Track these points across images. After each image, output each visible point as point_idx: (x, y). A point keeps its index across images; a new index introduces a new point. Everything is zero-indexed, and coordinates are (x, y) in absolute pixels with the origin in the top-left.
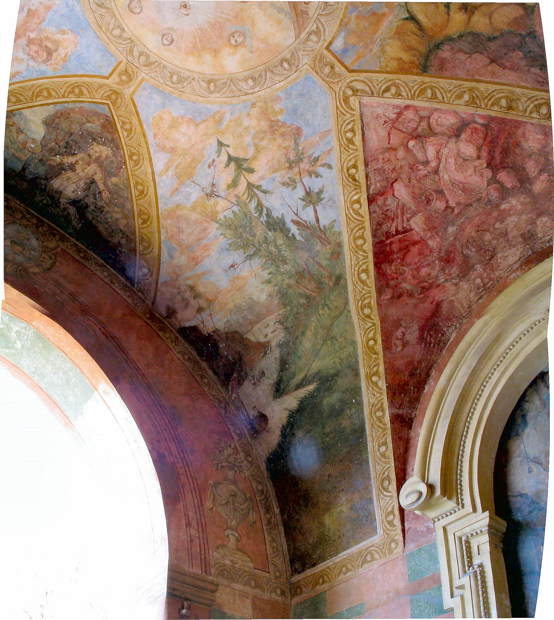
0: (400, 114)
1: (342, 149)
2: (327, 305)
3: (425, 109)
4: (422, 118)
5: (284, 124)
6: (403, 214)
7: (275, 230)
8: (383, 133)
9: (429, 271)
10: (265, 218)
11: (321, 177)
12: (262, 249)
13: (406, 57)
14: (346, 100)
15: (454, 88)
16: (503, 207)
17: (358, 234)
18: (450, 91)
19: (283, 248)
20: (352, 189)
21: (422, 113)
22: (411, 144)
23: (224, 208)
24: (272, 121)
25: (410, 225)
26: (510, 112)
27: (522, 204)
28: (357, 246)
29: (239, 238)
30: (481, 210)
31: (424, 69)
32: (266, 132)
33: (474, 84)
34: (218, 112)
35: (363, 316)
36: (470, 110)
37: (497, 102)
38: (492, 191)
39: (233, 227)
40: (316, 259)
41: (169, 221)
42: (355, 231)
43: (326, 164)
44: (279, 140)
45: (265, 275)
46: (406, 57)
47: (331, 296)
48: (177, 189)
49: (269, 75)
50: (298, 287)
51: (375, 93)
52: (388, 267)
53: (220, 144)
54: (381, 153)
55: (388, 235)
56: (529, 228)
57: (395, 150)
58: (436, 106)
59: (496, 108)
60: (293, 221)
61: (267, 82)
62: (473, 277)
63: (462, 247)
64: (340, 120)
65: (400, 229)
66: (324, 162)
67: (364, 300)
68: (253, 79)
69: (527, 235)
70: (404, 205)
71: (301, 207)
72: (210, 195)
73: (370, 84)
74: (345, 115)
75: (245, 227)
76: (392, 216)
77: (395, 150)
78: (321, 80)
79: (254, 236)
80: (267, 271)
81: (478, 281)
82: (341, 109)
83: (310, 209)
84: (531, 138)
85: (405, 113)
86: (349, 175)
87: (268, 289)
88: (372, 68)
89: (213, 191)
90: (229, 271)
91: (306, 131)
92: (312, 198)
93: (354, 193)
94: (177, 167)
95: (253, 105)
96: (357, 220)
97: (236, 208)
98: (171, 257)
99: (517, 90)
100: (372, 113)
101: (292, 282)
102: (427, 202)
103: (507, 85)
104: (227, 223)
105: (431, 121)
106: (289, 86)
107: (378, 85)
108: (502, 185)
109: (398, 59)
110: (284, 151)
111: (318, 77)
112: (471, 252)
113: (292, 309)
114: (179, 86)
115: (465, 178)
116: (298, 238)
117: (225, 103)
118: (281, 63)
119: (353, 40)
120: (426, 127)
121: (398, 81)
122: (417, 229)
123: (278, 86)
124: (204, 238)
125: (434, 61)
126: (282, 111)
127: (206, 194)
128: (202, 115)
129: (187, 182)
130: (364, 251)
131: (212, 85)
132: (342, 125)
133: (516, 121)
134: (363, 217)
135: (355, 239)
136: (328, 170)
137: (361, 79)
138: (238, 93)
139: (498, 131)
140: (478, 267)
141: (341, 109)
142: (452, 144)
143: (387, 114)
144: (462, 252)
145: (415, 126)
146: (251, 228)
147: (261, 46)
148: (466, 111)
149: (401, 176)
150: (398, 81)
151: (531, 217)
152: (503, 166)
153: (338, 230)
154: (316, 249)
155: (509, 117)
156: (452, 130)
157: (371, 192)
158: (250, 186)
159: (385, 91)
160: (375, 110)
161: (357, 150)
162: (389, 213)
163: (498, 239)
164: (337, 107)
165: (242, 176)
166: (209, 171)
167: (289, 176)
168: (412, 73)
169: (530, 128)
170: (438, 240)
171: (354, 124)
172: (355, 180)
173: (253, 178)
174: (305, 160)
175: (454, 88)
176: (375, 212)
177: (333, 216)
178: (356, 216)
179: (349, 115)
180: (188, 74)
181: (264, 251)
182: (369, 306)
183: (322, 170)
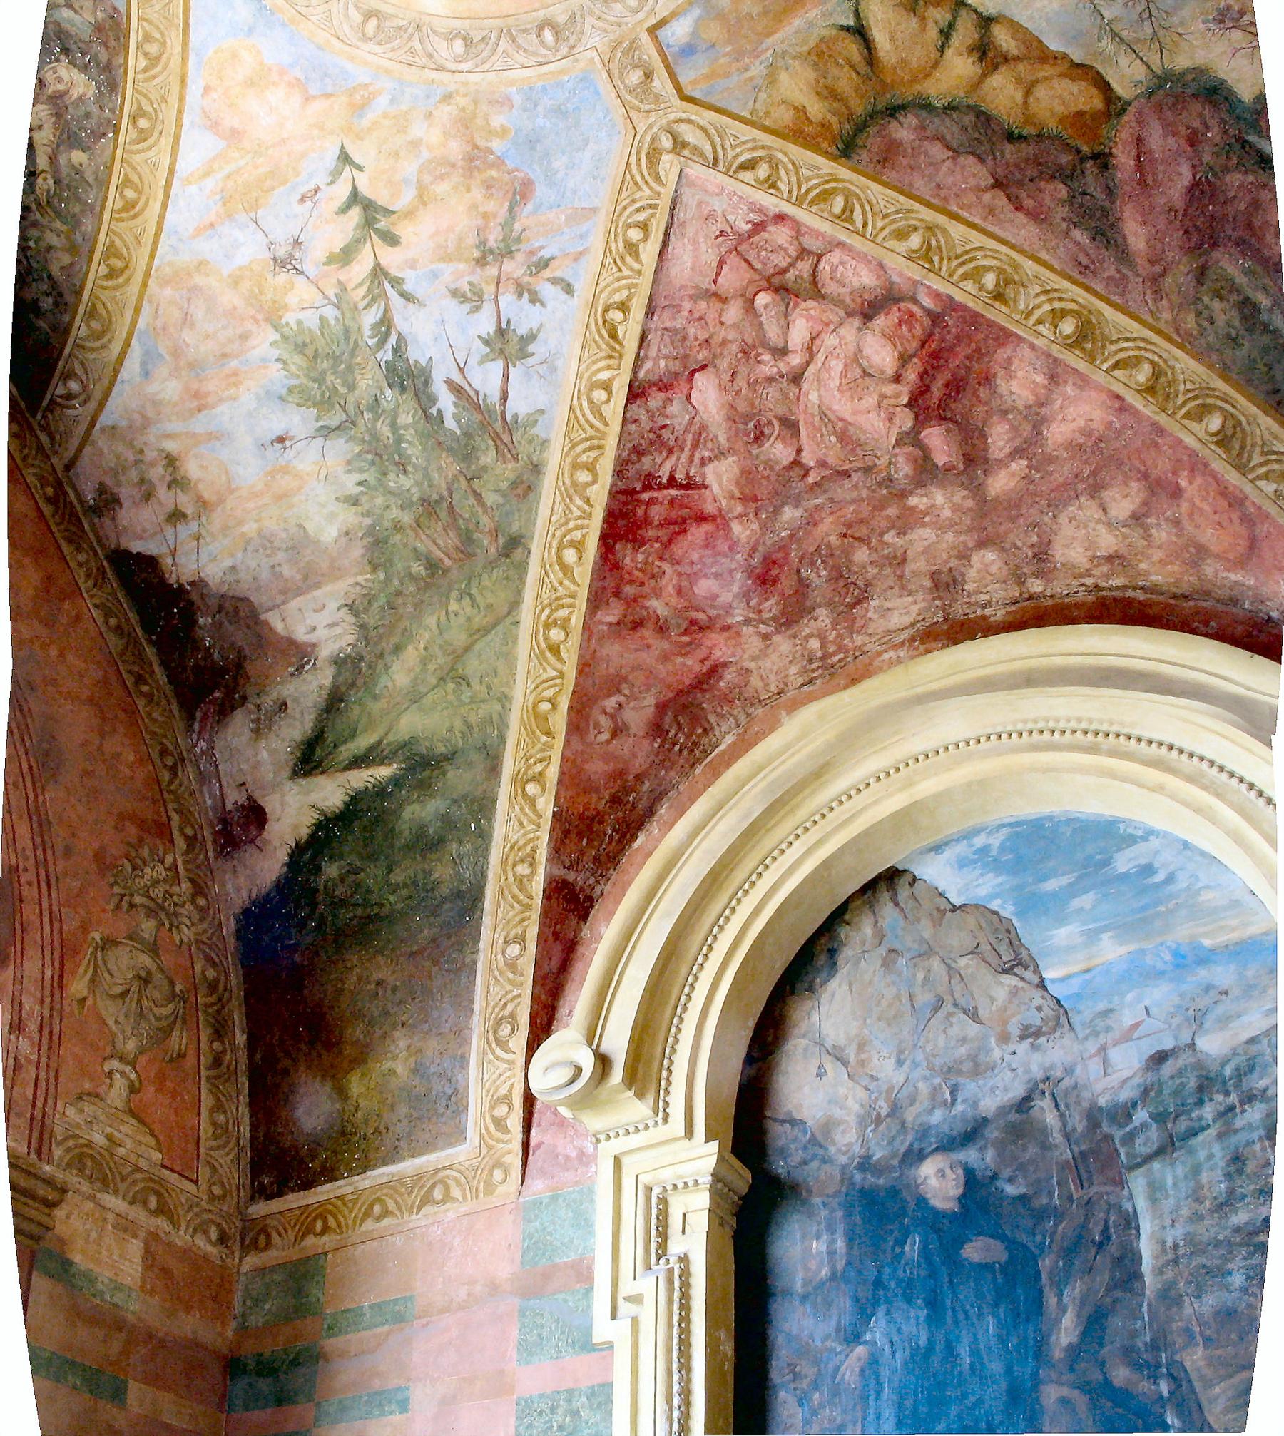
0: (758, 227)
1: (609, 259)
3: (818, 234)
4: (803, 252)
5: (499, 163)
6: (695, 446)
7: (403, 389)
10: (389, 356)
11: (543, 304)
12: (361, 422)
13: (817, 109)
14: (653, 156)
15: (897, 212)
16: (913, 501)
17: (584, 458)
18: (884, 216)
19: (409, 434)
20: (603, 354)
21: (809, 242)
22: (763, 299)
23: (304, 304)
24: (476, 147)
25: (704, 476)
26: (997, 305)
27: (956, 508)
28: (574, 484)
29: (315, 381)
30: (864, 493)
31: (846, 149)
32: (453, 166)
33: (941, 219)
36: (915, 272)
37: (975, 275)
38: (900, 459)
39: (309, 351)
41: (168, 292)
42: (579, 449)
43: (562, 280)
44: (477, 194)
45: (350, 484)
46: (817, 109)
47: (485, 576)
48: (212, 225)
49: (504, 44)
51: (721, 164)
52: (629, 551)
53: (345, 158)
54: (691, 297)
55: (650, 482)
56: (953, 563)
57: (724, 300)
58: (843, 236)
59: (969, 286)
60: (449, 383)
61: (494, 58)
62: (807, 631)
63: (801, 559)
64: (625, 194)
65: (680, 476)
66: (558, 274)
68: (468, 41)
69: (944, 578)
70: (703, 427)
72: (281, 263)
73: (717, 139)
74: (640, 189)
75: (336, 359)
76: (671, 443)
77: (724, 300)
78: (614, 95)
79: (351, 387)
80: (357, 477)
81: (815, 644)
84: (1020, 374)
85: (771, 228)
86: (605, 322)
87: (349, 517)
88: (734, 107)
89: (291, 256)
90: (270, 449)
91: (541, 192)
92: (507, 345)
93: (602, 364)
94: (228, 177)
96: (592, 426)
97: (330, 313)
98: (146, 374)
99: (1029, 266)
100: (700, 203)
101: (407, 518)
102: (756, 439)
103: (1013, 247)
104: (300, 340)
105: (821, 266)
106: (540, 84)
107: (733, 147)
108: (926, 455)
109: (796, 108)
110: (480, 222)
111: (610, 87)
112: (818, 577)
113: (388, 580)
115: (855, 413)
116: (450, 423)
118: (541, 28)
119: (714, 31)
120: (806, 274)
121: (780, 155)
122: (715, 488)
123: (515, 73)
124: (237, 356)
125: (872, 140)
126: (504, 131)
127: (275, 259)
128: (327, 80)
129: (242, 217)
130: (587, 501)
131: (373, 23)
132: (625, 208)
133: (1002, 328)
134: (606, 424)
135: (575, 466)
136: (564, 296)
137: (703, 123)
139: (958, 338)
140: (823, 614)
143: (731, 218)
144: (798, 571)
145: (784, 264)
146: (350, 368)
148: (903, 270)
149: (717, 362)
150: (780, 155)
151: (965, 543)
152: (941, 414)
153: (543, 435)
154: (482, 462)
155: (990, 315)
156: (859, 300)
157: (641, 375)
158: (379, 272)
159: (743, 167)
160: (708, 199)
161: (639, 273)
162: (666, 434)
163: (882, 567)
165: (368, 245)
166: (298, 209)
168: (816, 149)
169: (1025, 351)
171: (653, 215)
172: (613, 335)
173: (391, 258)
174: (520, 257)
175: (897, 212)
177: (541, 401)
178: (591, 418)
179: (647, 192)
181: (363, 429)
183: (548, 291)
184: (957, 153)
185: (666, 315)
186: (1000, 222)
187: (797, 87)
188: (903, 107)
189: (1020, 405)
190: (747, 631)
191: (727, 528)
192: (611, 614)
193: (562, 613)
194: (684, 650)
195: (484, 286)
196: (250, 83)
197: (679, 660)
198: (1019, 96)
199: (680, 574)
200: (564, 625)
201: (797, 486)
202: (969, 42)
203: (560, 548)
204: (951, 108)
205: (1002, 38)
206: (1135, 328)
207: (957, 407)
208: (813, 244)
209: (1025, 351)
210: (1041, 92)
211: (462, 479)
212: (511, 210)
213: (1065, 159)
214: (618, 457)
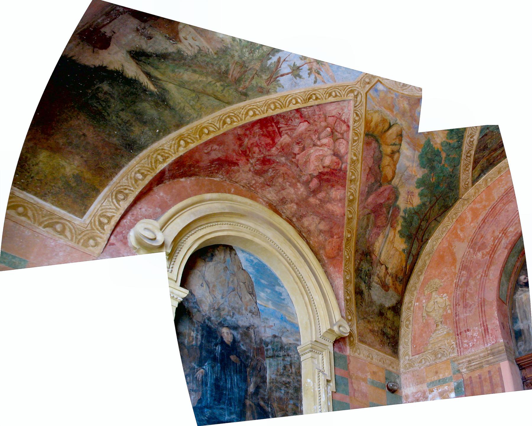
0: (344, 122)
3: (348, 136)
4: (342, 134)
6: (289, 130)
8: (334, 113)
17: (277, 104)
21: (345, 134)
22: (329, 129)
25: (284, 135)
30: (295, 173)
33: (360, 161)
36: (349, 161)
37: (353, 174)
38: (307, 177)
42: (279, 102)
55: (277, 123)
63: (273, 167)
65: (281, 129)
66: (318, 78)
70: (295, 129)
77: (325, 121)
83: (289, 70)
85: (345, 125)
99: (358, 183)
100: (345, 106)
108: (310, 182)
115: (312, 162)
122: (282, 139)
130: (267, 111)
142: (330, 152)
143: (344, 114)
162: (290, 121)
170: (276, 153)
177: (286, 86)
178: (288, 102)
183: (313, 77)
185: (318, 109)
191: (273, 147)
201: (290, 157)
206: (356, 210)
207: (325, 184)
209: (343, 192)
213: (379, 178)
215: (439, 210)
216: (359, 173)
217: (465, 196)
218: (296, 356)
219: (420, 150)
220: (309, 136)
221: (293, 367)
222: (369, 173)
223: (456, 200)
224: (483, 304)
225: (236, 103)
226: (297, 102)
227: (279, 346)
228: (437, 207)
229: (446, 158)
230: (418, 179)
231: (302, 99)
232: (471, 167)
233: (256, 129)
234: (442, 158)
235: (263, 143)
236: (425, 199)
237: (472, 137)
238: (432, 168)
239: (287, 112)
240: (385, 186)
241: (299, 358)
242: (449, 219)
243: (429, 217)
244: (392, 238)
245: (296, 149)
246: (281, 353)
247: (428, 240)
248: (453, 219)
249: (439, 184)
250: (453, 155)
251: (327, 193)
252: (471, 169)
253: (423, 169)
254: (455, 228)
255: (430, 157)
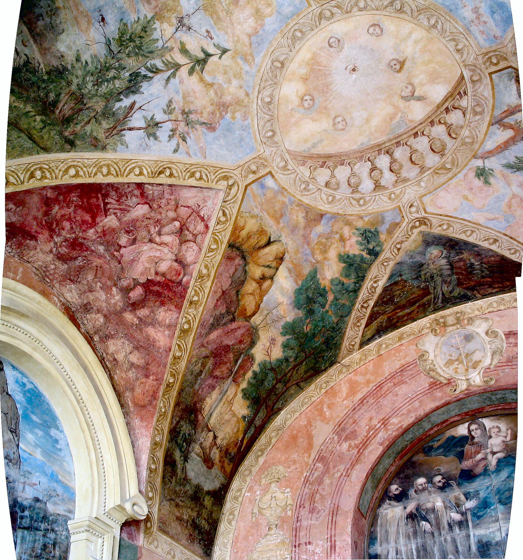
1: (188, 166)
2: (45, 127)
5: (222, 117)
6: (121, 209)
9: (66, 229)
12: (112, 62)
14: (226, 178)
16: (114, 289)
17: (112, 169)
22: (177, 224)
24: (228, 107)
25: (110, 215)
27: (115, 304)
28: (101, 167)
33: (212, 278)
34: (254, 60)
35: (32, 169)
36: (195, 274)
37: (197, 294)
38: (128, 281)
40: (93, 120)
42: (115, 166)
44: (210, 109)
49: (267, 117)
50: (67, 94)
52: (77, 194)
53: (225, 51)
54: (176, 198)
55: (106, 195)
56: (95, 308)
59: (193, 293)
60: (134, 103)
61: (262, 114)
63: (85, 256)
64: (212, 169)
65: (109, 206)
66: (181, 146)
67: (49, 172)
68: (270, 103)
69: (89, 307)
70: (128, 211)
71: (146, 115)
82: (220, 171)
86: (165, 168)
89: (183, 25)
91: (211, 135)
92: (152, 127)
95: (247, 95)
96: (125, 170)
99: (201, 308)
103: (206, 302)
106: (251, 131)
110: (199, 111)
112: (79, 262)
114: (291, 34)
115: (142, 262)
116: (118, 105)
117: (259, 70)
118: (272, 131)
122: (106, 220)
126: (234, 118)
128: (257, 45)
130: (95, 174)
131: (279, 65)
133: (182, 307)
134: (127, 176)
135: (108, 166)
138: (262, 86)
139: (175, 292)
141: (220, 171)
143: (205, 208)
145: (190, 229)
147: (293, 120)
153: (118, 149)
155: (185, 302)
157: (146, 186)
158: (177, 67)
160: (211, 200)
161: (184, 179)
162: (124, 198)
163: (87, 285)
164: (222, 168)
165: (188, 61)
167: (177, 109)
168: (231, 235)
170: (94, 237)
173: (184, 72)
174: (186, 128)
176: (129, 187)
177: (131, 146)
178: (128, 169)
179: (213, 177)
180: (297, 47)
182: (43, 177)
183: (174, 142)
184: (231, 277)
186: (213, 296)
187: (251, 225)
188: (245, 259)
189: (157, 317)
190: (52, 244)
191: (91, 227)
192: (50, 194)
193: (48, 175)
194: (40, 224)
195: (174, 115)
196: (258, 11)
197: (35, 223)
198: (250, 292)
199: (70, 214)
200: (43, 177)
201: (112, 249)
202: (265, 274)
203: (74, 166)
204: (245, 272)
205: (267, 283)
206: (189, 346)
207: (152, 298)
208: (199, 238)
209: (175, 315)
210: (251, 298)
211: (95, 113)
212: (204, 123)
213: (233, 309)
214: (115, 183)
215: (306, 372)
216: (206, 295)
217: (346, 361)
218: (64, 533)
219: (300, 282)
220: (147, 226)
221: (57, 548)
222: (220, 298)
223: (332, 364)
224: (335, 512)
225: (56, 152)
226: (141, 173)
227: (41, 515)
228: (303, 368)
229: (332, 302)
230: (287, 323)
231: (149, 170)
232: (364, 322)
233: (74, 197)
234: (327, 301)
235: (78, 218)
236: (290, 353)
237: (375, 282)
238: (311, 312)
239: (124, 184)
240: (240, 322)
241: (68, 537)
242: (316, 388)
243: (290, 380)
244: (231, 397)
245: (124, 240)
246: (43, 526)
247: (280, 410)
248: (321, 388)
249: (314, 335)
250: (344, 300)
251: (152, 312)
252: (363, 326)
253: (297, 311)
254: (321, 403)
255: (311, 295)
